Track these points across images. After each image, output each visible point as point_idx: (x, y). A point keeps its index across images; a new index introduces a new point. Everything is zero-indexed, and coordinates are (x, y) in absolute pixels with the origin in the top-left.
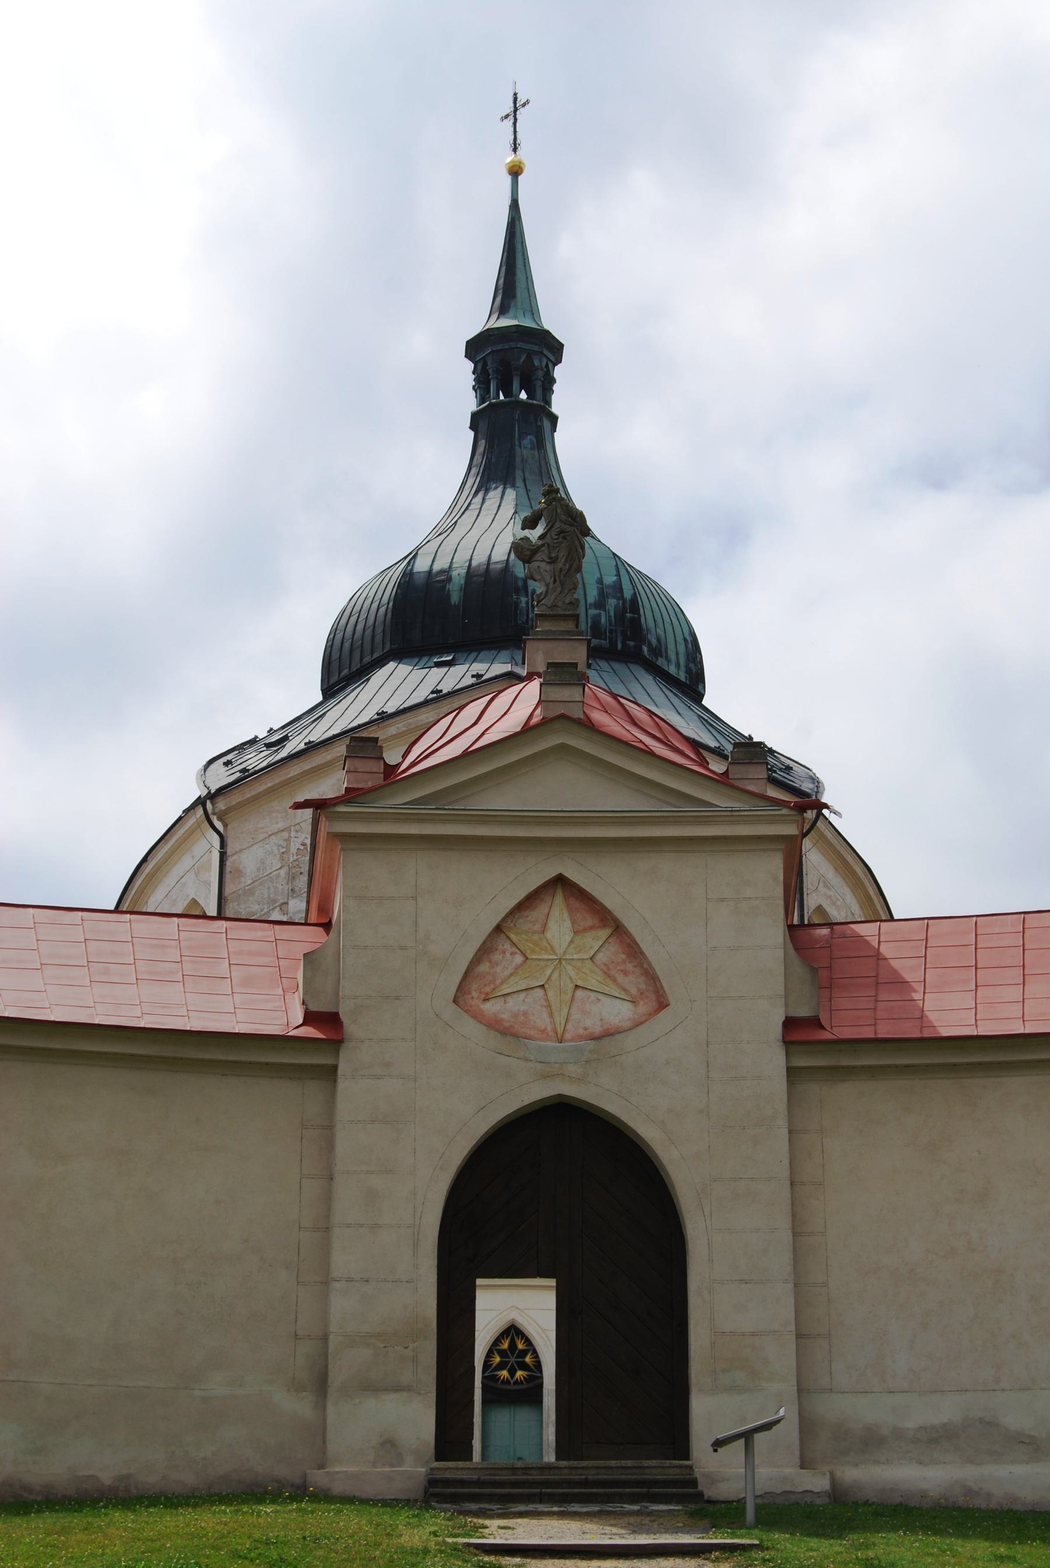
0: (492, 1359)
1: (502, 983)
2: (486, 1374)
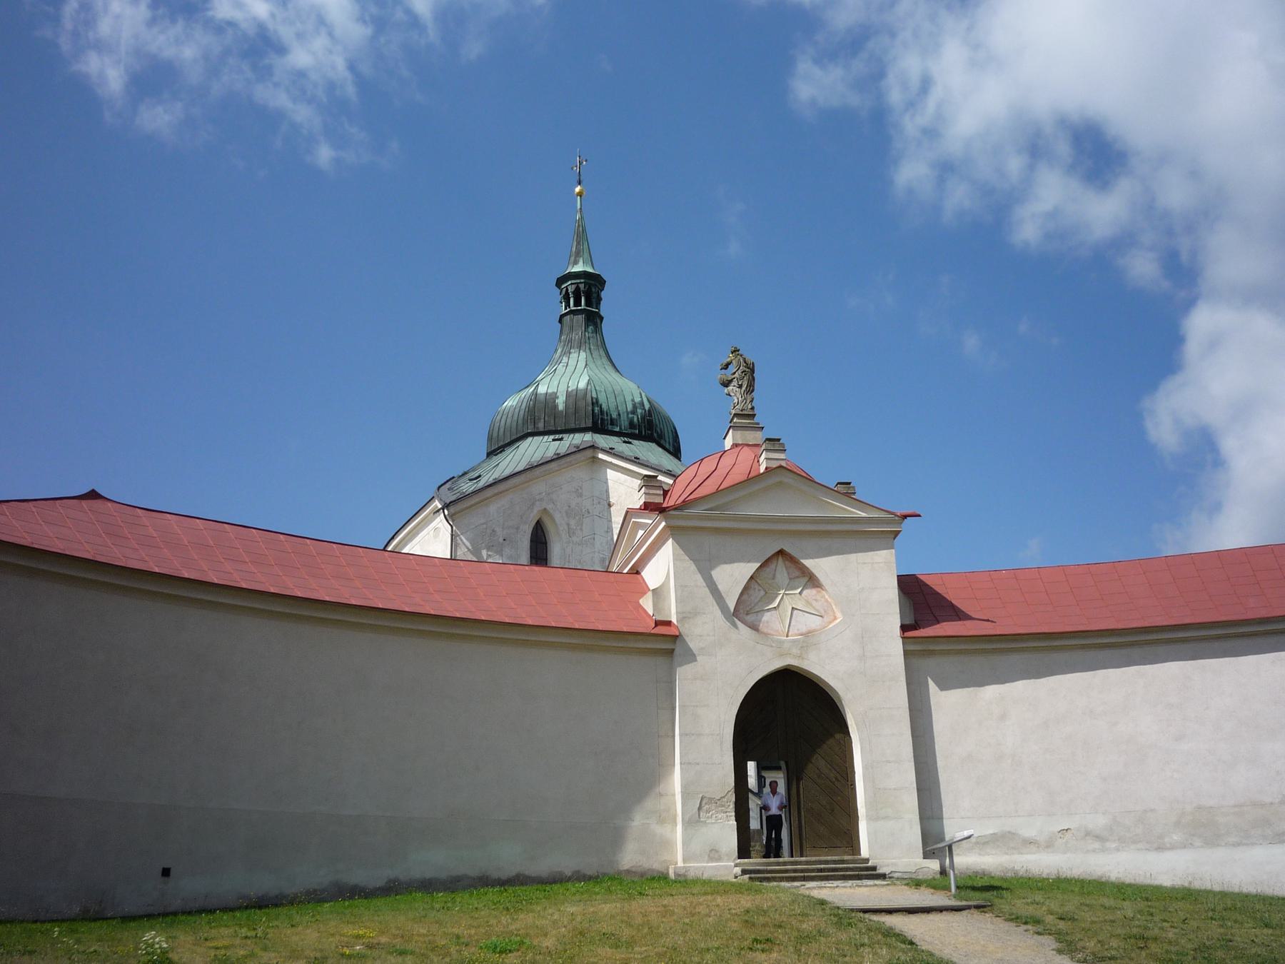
1: (755, 605)
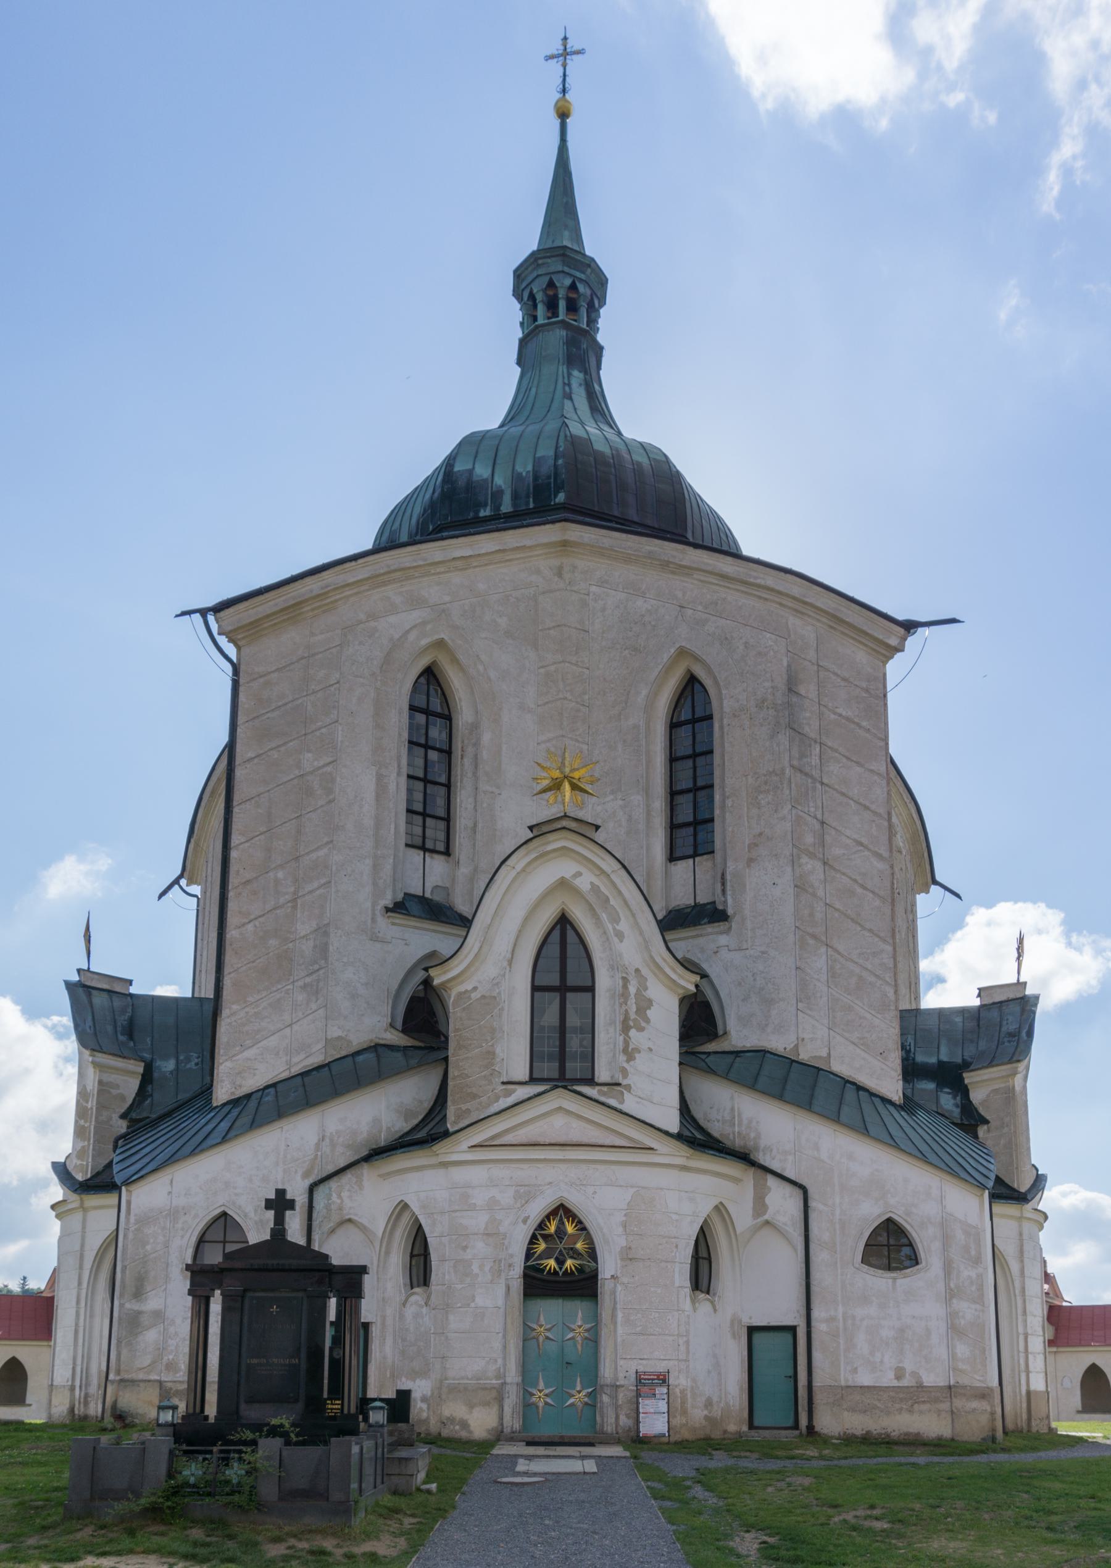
2: (528, 1264)
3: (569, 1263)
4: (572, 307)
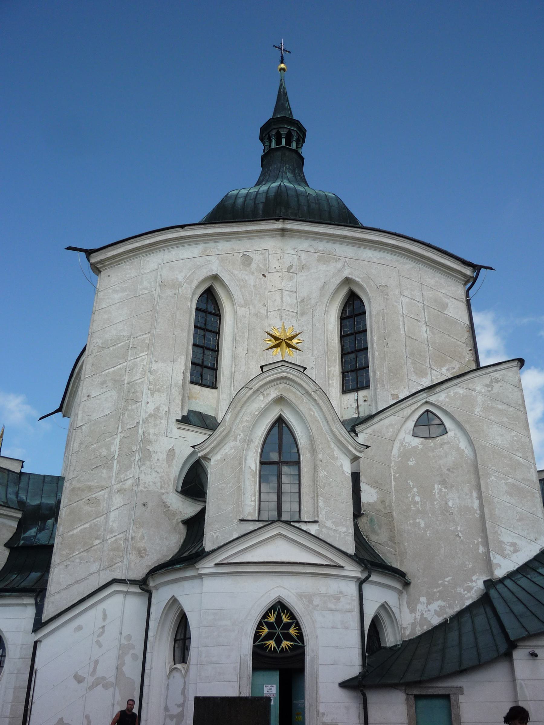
0: (261, 630)
2: (256, 644)
3: (285, 644)
4: (289, 143)
